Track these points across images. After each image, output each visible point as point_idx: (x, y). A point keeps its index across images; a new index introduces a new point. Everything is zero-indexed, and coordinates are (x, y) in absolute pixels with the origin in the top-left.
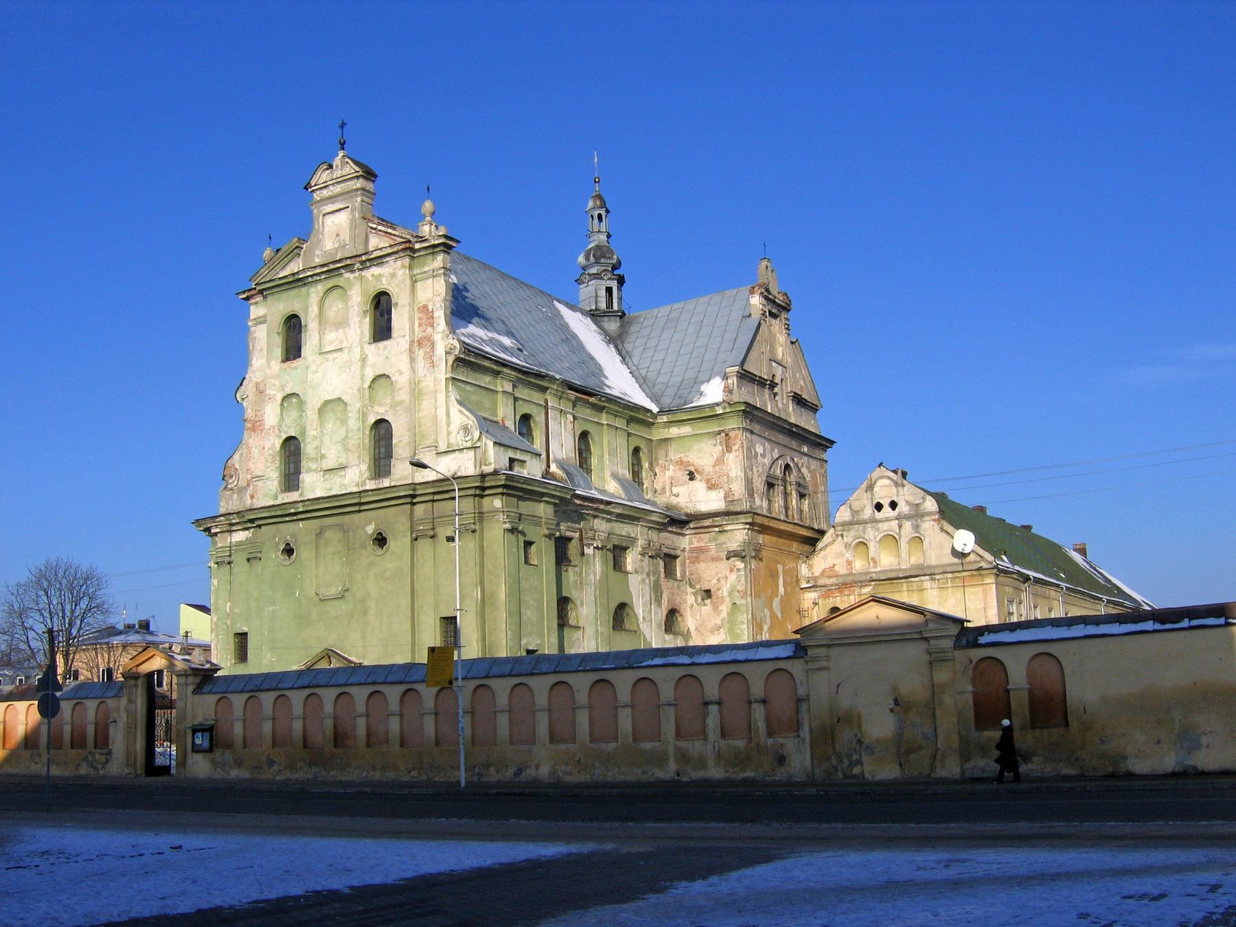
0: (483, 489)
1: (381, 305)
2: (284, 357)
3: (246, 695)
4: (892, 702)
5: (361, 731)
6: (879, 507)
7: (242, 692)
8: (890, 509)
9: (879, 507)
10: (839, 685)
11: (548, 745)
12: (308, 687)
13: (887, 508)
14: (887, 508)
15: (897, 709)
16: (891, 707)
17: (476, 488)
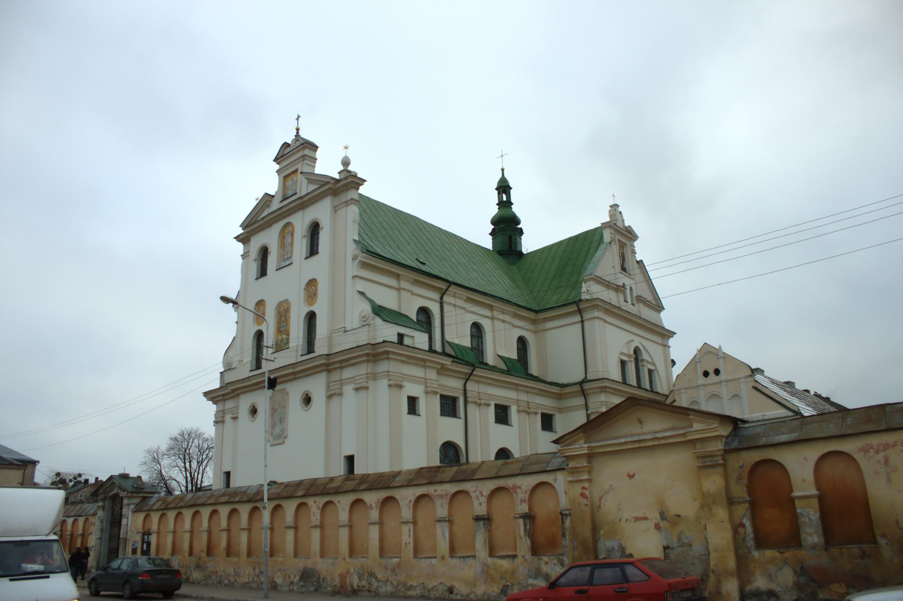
0: (375, 355)
1: (315, 229)
2: (260, 273)
3: (160, 513)
4: (658, 516)
5: (224, 544)
6: (706, 374)
7: (157, 510)
8: (714, 375)
9: (706, 374)
10: (601, 498)
11: (348, 559)
12: (193, 506)
13: (712, 374)
14: (712, 374)
15: (663, 524)
16: (657, 521)
17: (368, 355)
